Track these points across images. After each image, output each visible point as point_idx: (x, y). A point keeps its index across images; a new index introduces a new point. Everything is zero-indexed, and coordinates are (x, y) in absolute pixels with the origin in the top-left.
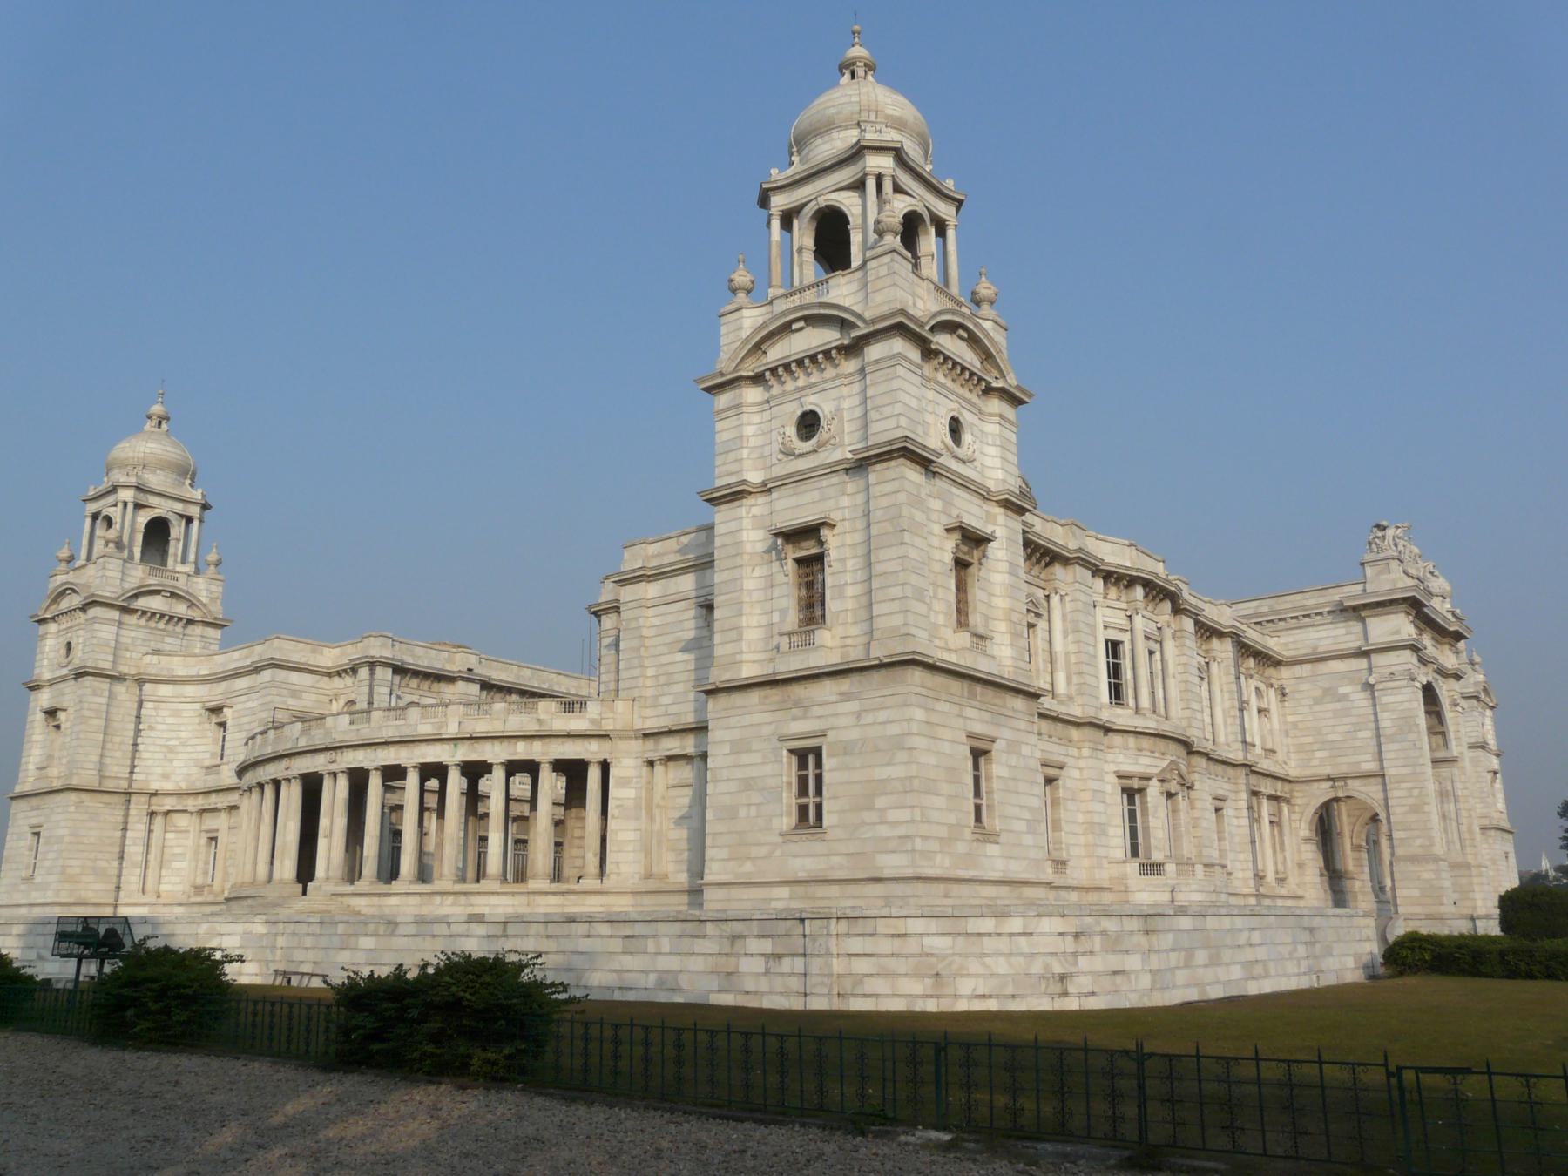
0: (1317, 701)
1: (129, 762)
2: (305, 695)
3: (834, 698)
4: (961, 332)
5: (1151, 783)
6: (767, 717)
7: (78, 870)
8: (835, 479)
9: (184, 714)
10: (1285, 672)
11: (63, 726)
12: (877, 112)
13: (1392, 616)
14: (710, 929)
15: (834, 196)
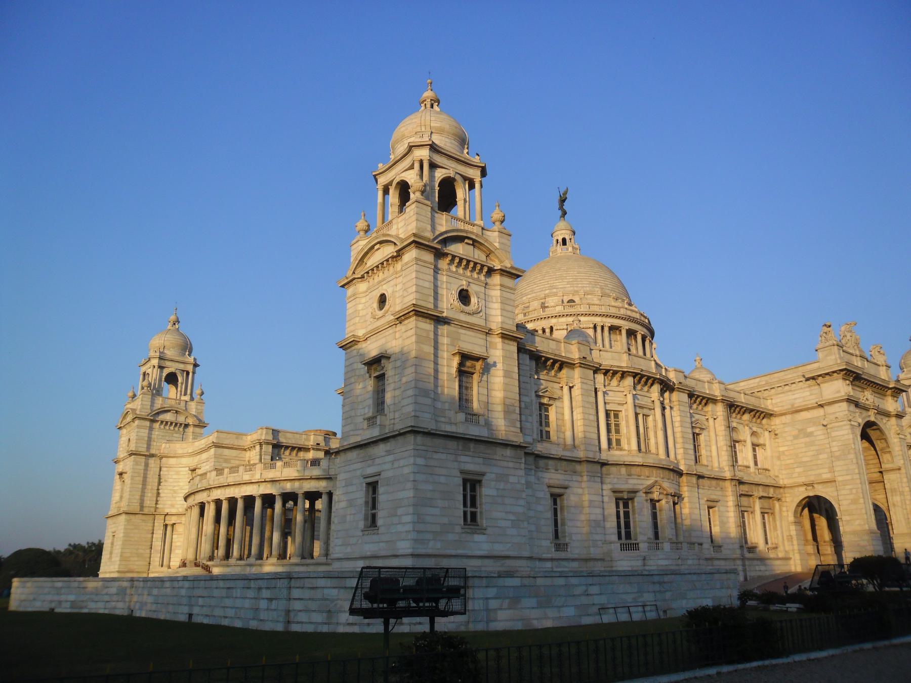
0: (796, 437)
1: (155, 499)
2: (233, 461)
3: (384, 454)
4: (466, 241)
5: (638, 494)
6: (359, 465)
7: (129, 555)
8: (391, 331)
9: (182, 473)
10: (776, 421)
11: (125, 481)
12: (425, 126)
13: (836, 382)
14: (252, 584)
15: (403, 174)
